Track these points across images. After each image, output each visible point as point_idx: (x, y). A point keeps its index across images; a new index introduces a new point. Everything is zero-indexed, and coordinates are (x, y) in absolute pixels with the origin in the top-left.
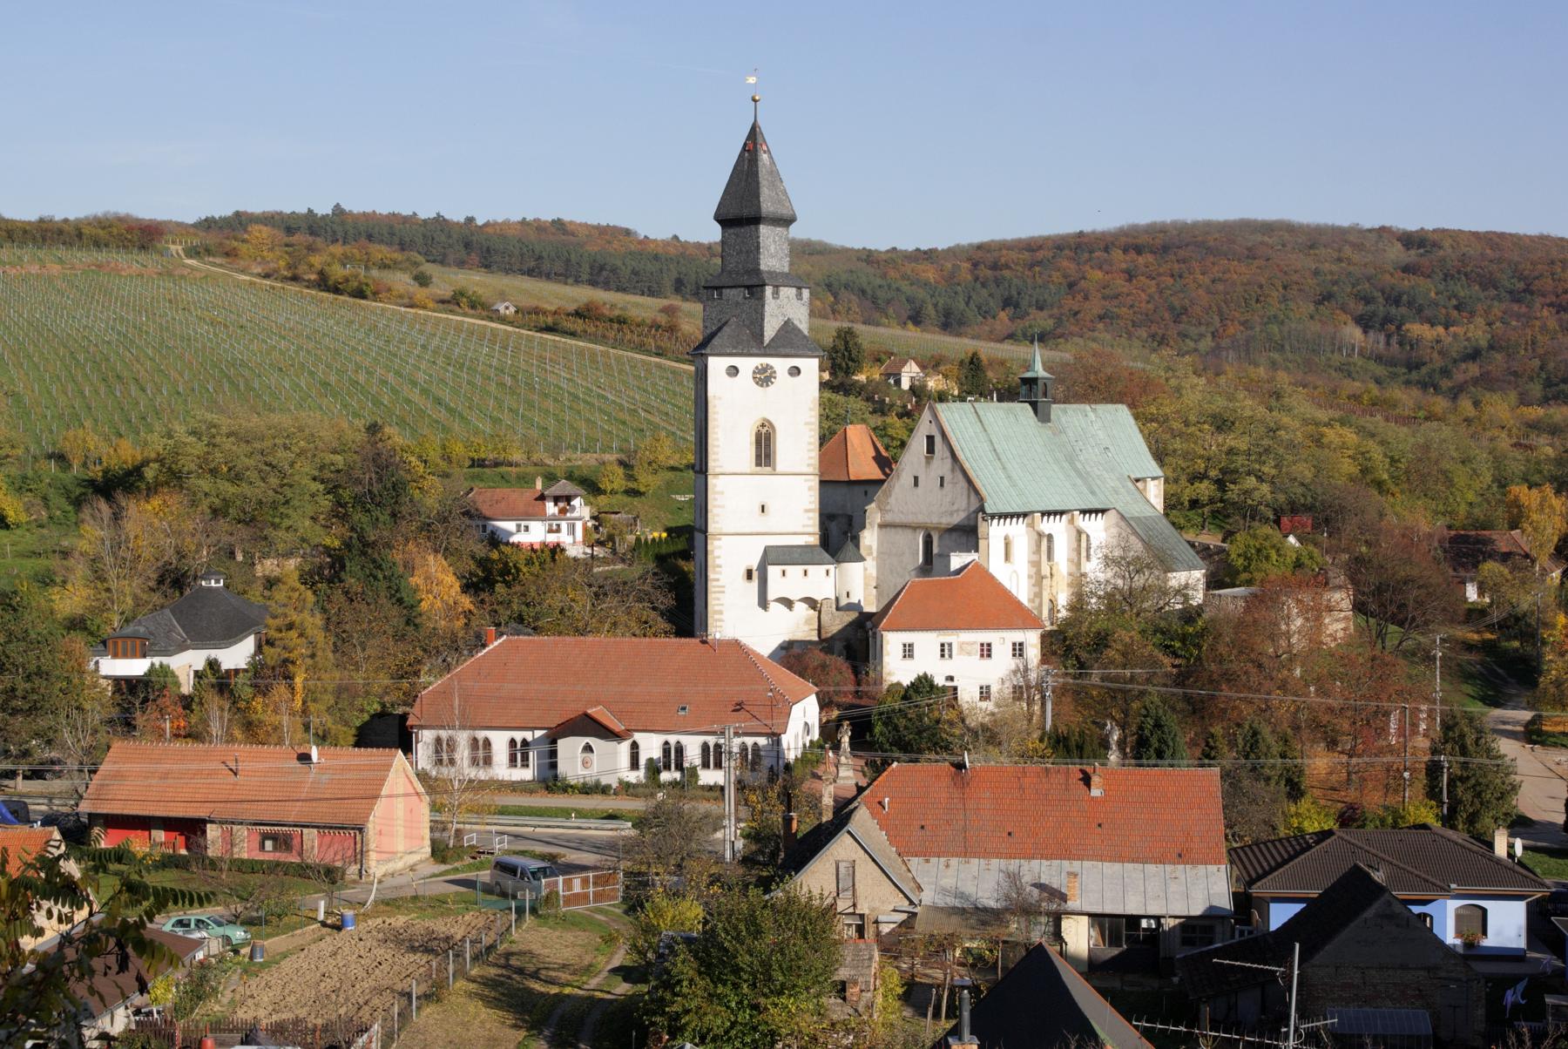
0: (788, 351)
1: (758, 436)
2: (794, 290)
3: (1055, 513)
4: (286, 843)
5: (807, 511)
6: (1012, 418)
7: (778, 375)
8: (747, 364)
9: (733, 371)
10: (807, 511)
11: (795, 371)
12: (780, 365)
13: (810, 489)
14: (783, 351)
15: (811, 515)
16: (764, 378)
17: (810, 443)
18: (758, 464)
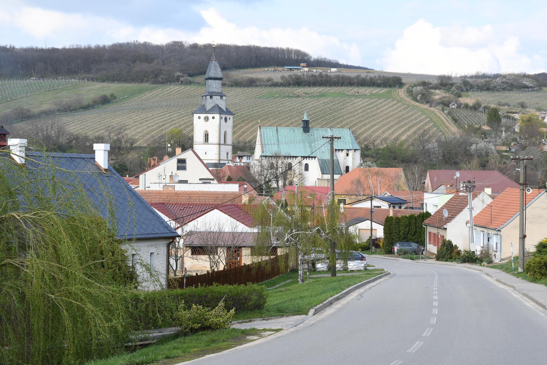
0: (212, 112)
1: (206, 134)
2: (219, 97)
3: (293, 157)
4: (445, 244)
5: (216, 154)
6: (292, 131)
7: (210, 119)
8: (203, 116)
9: (199, 118)
10: (216, 154)
11: (213, 118)
12: (210, 116)
13: (216, 148)
14: (210, 112)
15: (217, 155)
16: (207, 119)
17: (217, 136)
18: (206, 142)
